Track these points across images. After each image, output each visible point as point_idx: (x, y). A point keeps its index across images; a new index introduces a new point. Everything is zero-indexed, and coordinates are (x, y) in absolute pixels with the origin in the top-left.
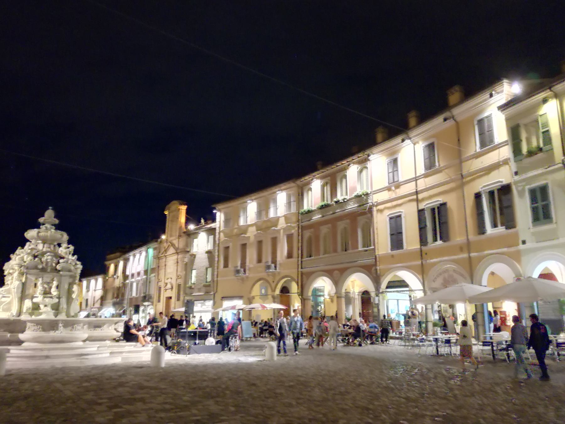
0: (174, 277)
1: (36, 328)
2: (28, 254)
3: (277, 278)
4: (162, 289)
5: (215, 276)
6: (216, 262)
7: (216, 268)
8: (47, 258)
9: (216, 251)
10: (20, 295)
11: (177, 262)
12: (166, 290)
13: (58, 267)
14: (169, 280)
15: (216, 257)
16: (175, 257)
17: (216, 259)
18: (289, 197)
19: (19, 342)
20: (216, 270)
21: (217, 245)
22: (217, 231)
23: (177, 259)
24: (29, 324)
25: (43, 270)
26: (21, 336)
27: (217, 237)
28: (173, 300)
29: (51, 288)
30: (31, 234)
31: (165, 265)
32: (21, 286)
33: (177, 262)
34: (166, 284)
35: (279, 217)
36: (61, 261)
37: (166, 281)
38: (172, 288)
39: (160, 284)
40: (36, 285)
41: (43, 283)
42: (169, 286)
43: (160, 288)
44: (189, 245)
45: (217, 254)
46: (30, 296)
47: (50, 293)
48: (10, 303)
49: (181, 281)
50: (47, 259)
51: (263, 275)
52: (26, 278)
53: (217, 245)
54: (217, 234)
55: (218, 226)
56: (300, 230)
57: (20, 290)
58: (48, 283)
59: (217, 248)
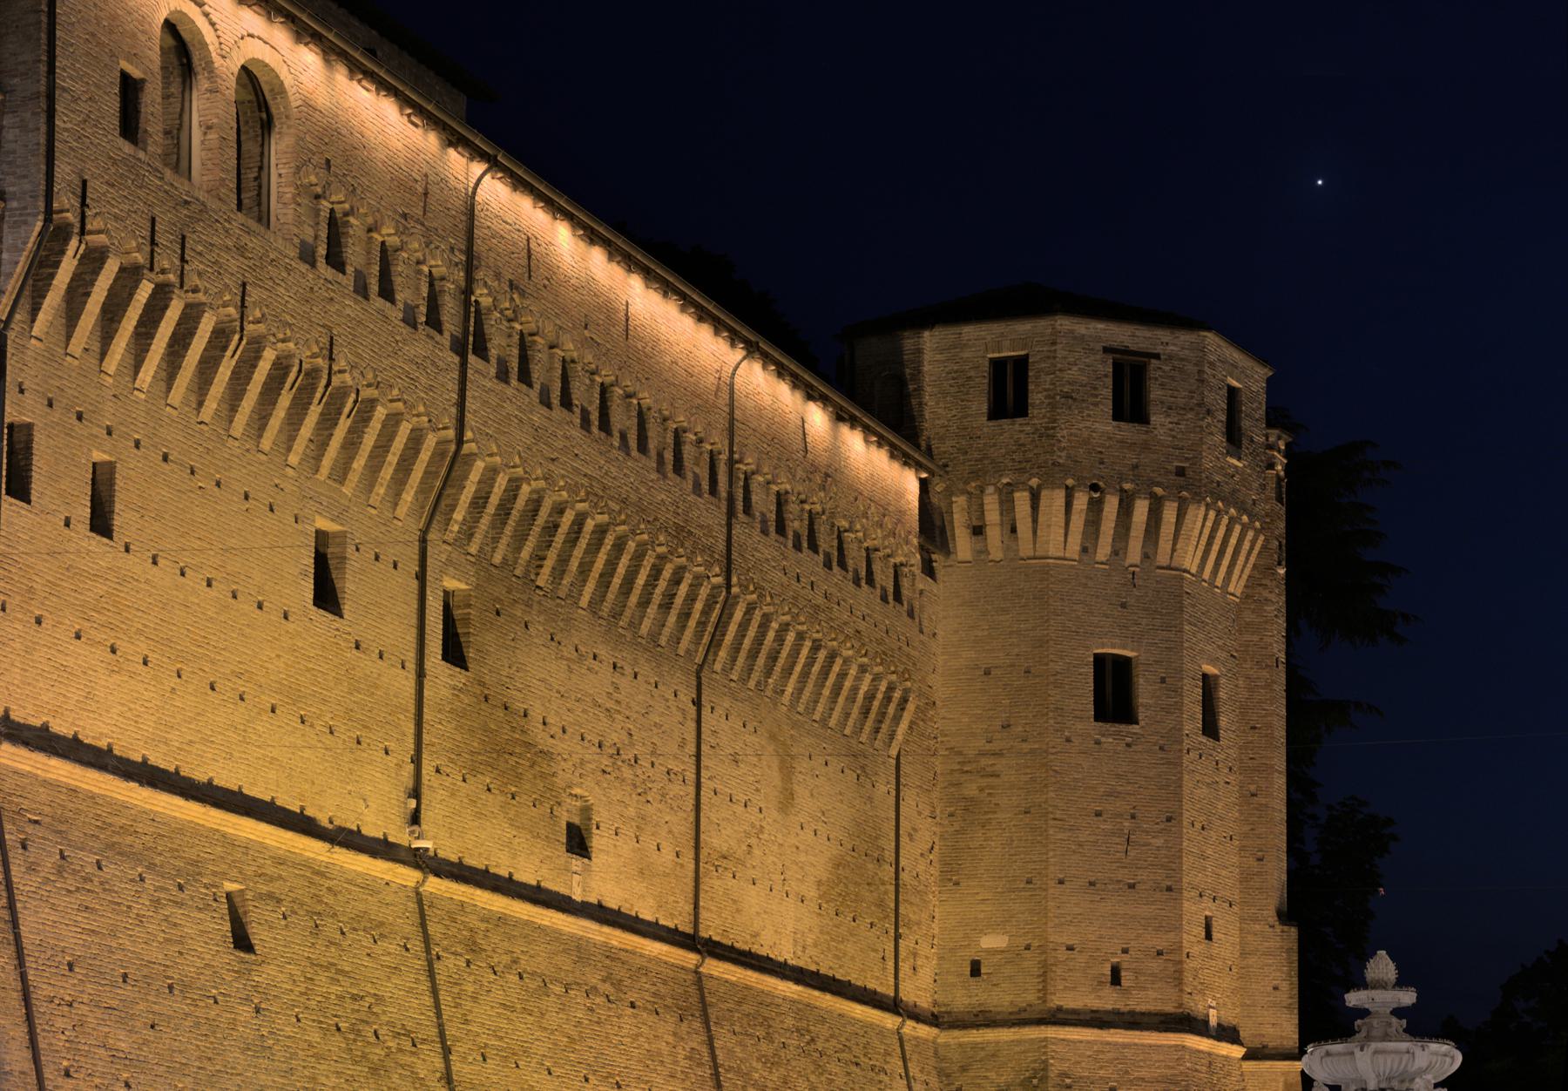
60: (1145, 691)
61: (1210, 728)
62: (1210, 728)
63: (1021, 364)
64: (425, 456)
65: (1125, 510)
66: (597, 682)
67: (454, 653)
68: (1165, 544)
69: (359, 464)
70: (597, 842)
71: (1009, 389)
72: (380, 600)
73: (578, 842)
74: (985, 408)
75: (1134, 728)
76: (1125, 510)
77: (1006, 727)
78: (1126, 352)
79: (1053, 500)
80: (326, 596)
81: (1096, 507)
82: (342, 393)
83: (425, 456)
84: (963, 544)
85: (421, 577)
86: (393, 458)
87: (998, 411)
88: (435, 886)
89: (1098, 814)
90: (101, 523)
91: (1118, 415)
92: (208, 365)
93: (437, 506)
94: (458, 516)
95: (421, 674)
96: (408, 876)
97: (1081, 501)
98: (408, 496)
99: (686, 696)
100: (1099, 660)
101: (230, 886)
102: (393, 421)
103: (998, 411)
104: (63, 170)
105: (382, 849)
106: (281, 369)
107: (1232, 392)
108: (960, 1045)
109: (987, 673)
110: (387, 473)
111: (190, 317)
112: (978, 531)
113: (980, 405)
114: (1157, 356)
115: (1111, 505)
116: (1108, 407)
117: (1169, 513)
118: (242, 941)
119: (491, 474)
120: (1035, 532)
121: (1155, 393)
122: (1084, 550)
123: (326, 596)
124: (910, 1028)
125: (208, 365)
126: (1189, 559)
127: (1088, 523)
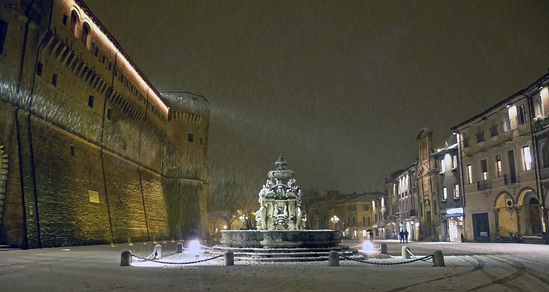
0: (430, 195)
1: (268, 237)
3: (518, 191)
4: (423, 205)
5: (462, 192)
6: (461, 179)
7: (462, 184)
9: (461, 169)
11: (431, 182)
12: (425, 206)
14: (427, 197)
15: (461, 174)
16: (428, 178)
17: (461, 177)
18: (520, 110)
19: (262, 247)
20: (462, 186)
21: (460, 164)
22: (459, 151)
23: (430, 179)
25: (277, 198)
27: (460, 156)
28: (432, 214)
31: (423, 185)
33: (431, 182)
34: (425, 201)
35: (513, 130)
36: (288, 191)
37: (425, 198)
38: (430, 205)
39: (421, 201)
40: (274, 208)
42: (427, 202)
43: (421, 204)
44: (437, 166)
45: (461, 172)
48: (260, 221)
49: (435, 198)
51: (504, 188)
52: (268, 204)
53: (460, 164)
54: (459, 154)
55: (459, 146)
56: (535, 141)
59: (460, 166)
62: (201, 143)
64: (107, 88)
66: (128, 126)
67: (109, 118)
69: (97, 86)
70: (128, 148)
72: (98, 106)
73: (125, 148)
76: (193, 116)
79: (184, 114)
80: (91, 105)
81: (189, 116)
82: (95, 75)
83: (107, 88)
84: (173, 119)
85: (105, 105)
86: (102, 87)
88: (104, 150)
90: (54, 83)
92: (74, 64)
93: (108, 97)
94: (111, 98)
95: (104, 119)
96: (100, 148)
97: (188, 115)
98: (104, 93)
99: (139, 131)
101: (71, 145)
102: (102, 82)
104: (52, 24)
105: (96, 143)
106: (86, 68)
110: (101, 89)
111: (72, 56)
112: (175, 117)
115: (191, 116)
118: (73, 154)
119: (116, 93)
123: (91, 105)
125: (74, 64)
126: (200, 123)
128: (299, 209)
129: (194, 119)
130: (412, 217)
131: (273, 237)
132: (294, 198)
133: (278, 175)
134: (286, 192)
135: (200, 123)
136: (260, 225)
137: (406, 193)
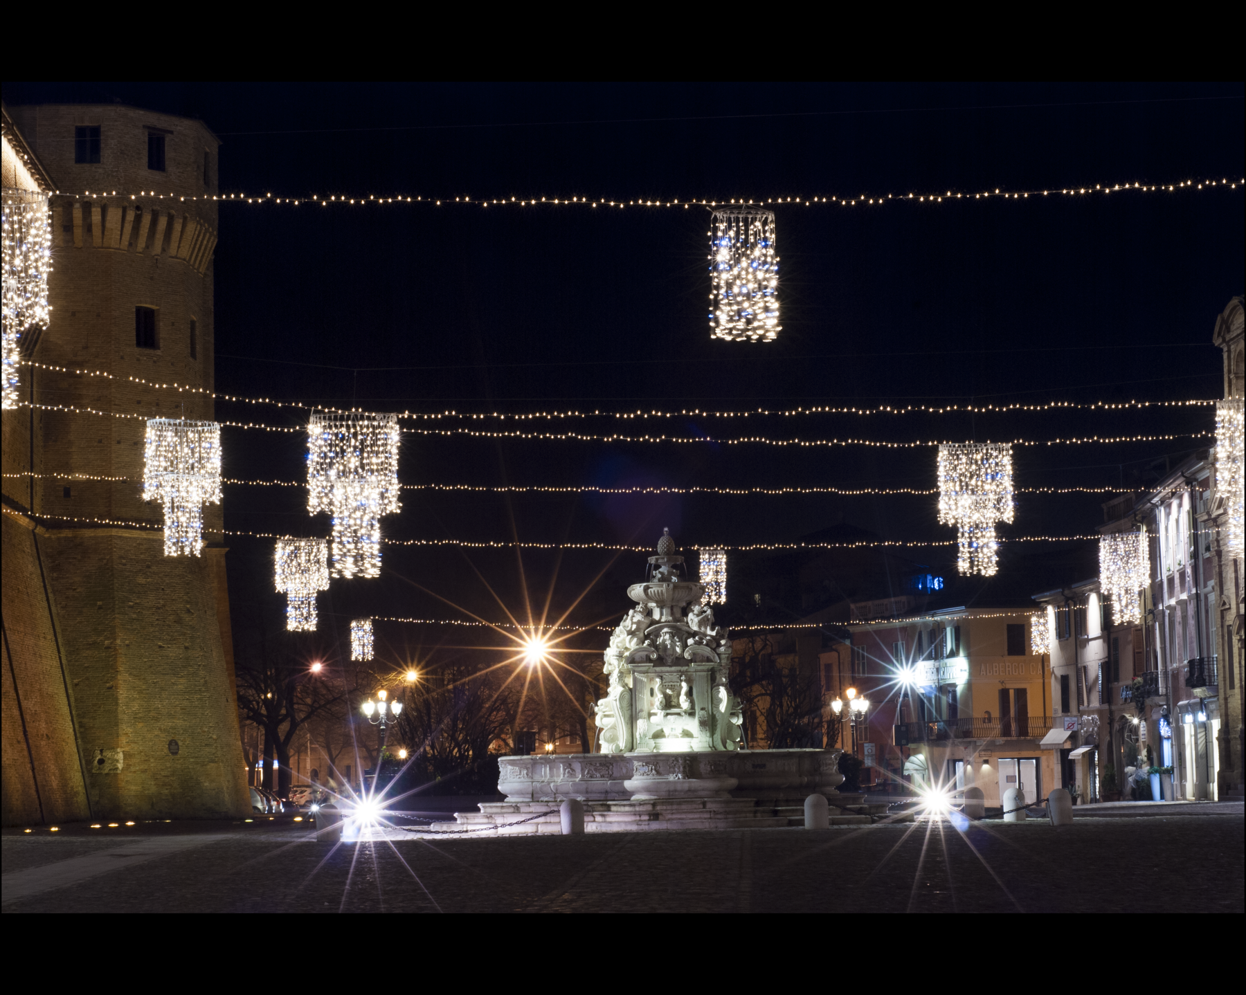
1: (646, 769)
2: (631, 633)
8: (665, 638)
10: (628, 714)
13: (686, 655)
24: (636, 763)
25: (660, 661)
26: (628, 784)
29: (679, 695)
30: (636, 591)
32: (627, 696)
36: (690, 641)
41: (663, 687)
46: (645, 714)
47: (678, 706)
48: (614, 727)
50: (664, 641)
52: (635, 680)
57: (626, 703)
58: (672, 688)
60: (163, 330)
61: (193, 355)
62: (193, 355)
63: (96, 131)
65: (154, 223)
68: (174, 245)
71: (88, 145)
74: (73, 156)
75: (159, 352)
76: (154, 223)
77: (86, 348)
78: (154, 128)
81: (138, 219)
87: (80, 159)
89: (139, 402)
91: (151, 166)
100: (139, 310)
103: (80, 159)
107: (206, 154)
108: (59, 539)
109: (74, 314)
113: (71, 154)
114: (171, 132)
116: (145, 160)
117: (178, 227)
120: (103, 233)
121: (169, 154)
122: (130, 244)
124: (39, 530)
126: (185, 252)
127: (133, 228)
128: (723, 693)
129: (160, 236)
130: (1198, 691)
131: (661, 770)
132: (709, 660)
133: (660, 594)
134: (685, 646)
135: (185, 252)
136: (613, 740)
137: (1182, 575)
